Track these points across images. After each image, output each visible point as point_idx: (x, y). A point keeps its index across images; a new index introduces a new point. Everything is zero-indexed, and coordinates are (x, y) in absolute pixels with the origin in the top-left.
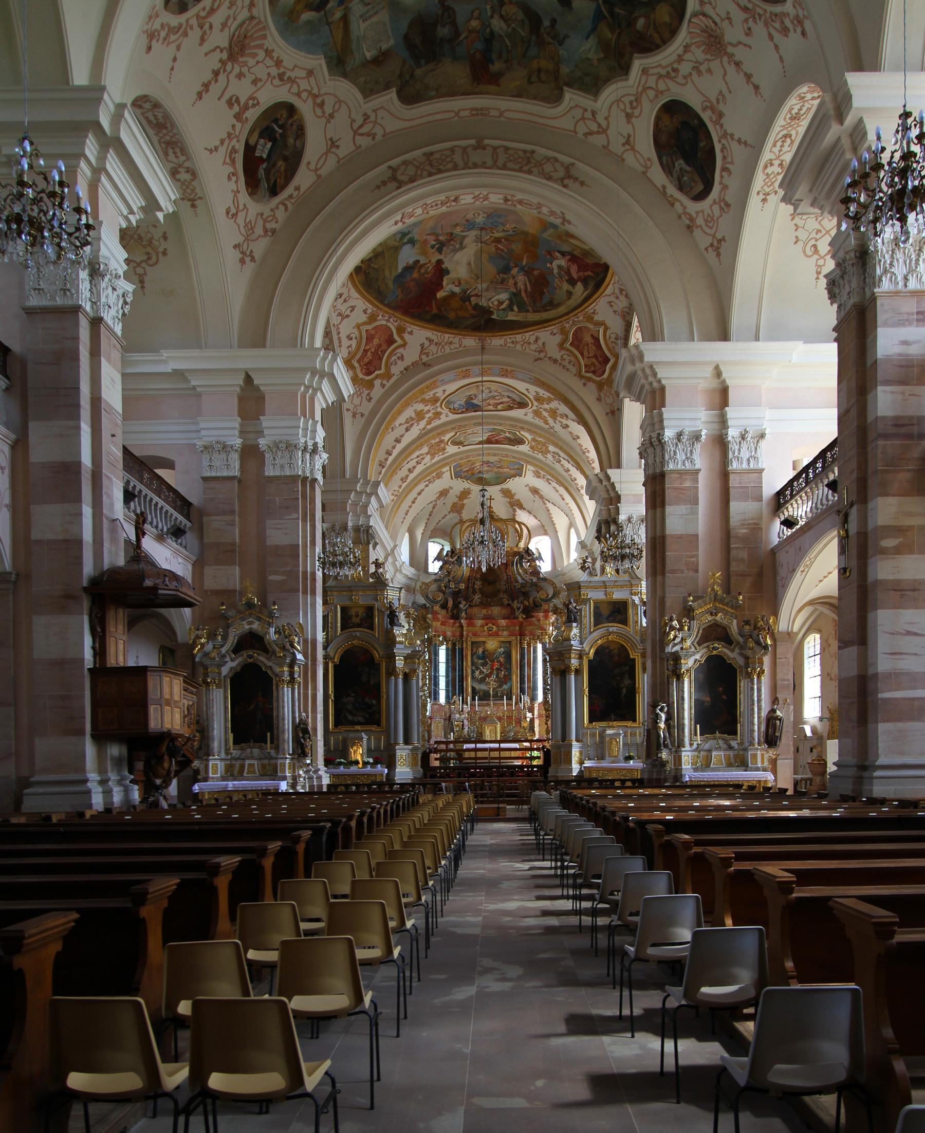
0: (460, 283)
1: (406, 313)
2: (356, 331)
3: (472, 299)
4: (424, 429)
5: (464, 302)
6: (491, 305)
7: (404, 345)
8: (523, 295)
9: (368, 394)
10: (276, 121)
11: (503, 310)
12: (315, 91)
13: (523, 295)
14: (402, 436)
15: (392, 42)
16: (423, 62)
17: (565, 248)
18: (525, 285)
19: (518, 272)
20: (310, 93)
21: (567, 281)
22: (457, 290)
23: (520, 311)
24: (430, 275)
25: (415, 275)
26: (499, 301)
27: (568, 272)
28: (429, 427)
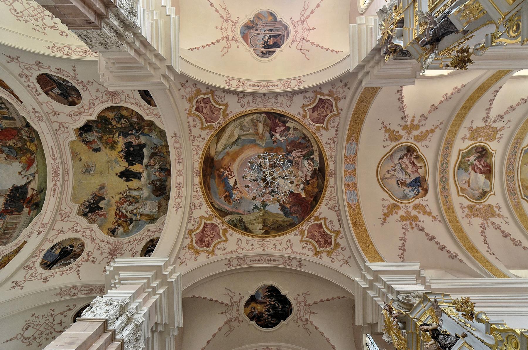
0: (298, 185)
1: (308, 214)
2: (303, 243)
3: (308, 179)
4: (434, 217)
5: (308, 184)
6: (311, 170)
7: (325, 219)
8: (304, 153)
9: (342, 248)
10: (149, 247)
11: (313, 163)
12: (155, 230)
13: (304, 153)
14: (427, 235)
15: (157, 201)
16: (165, 192)
17: (267, 134)
18: (298, 152)
19: (291, 156)
20: (154, 232)
21: (288, 132)
22: (302, 187)
23: (313, 154)
24: (291, 199)
25: (288, 206)
26: (309, 165)
27: (283, 131)
28: (435, 213)
